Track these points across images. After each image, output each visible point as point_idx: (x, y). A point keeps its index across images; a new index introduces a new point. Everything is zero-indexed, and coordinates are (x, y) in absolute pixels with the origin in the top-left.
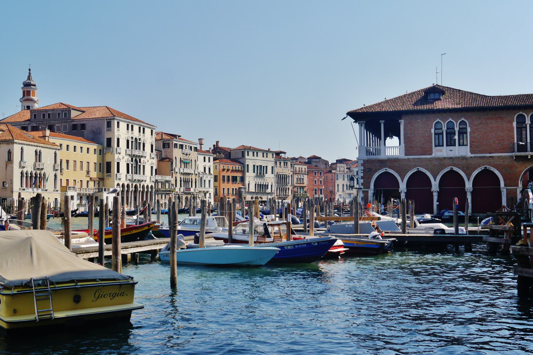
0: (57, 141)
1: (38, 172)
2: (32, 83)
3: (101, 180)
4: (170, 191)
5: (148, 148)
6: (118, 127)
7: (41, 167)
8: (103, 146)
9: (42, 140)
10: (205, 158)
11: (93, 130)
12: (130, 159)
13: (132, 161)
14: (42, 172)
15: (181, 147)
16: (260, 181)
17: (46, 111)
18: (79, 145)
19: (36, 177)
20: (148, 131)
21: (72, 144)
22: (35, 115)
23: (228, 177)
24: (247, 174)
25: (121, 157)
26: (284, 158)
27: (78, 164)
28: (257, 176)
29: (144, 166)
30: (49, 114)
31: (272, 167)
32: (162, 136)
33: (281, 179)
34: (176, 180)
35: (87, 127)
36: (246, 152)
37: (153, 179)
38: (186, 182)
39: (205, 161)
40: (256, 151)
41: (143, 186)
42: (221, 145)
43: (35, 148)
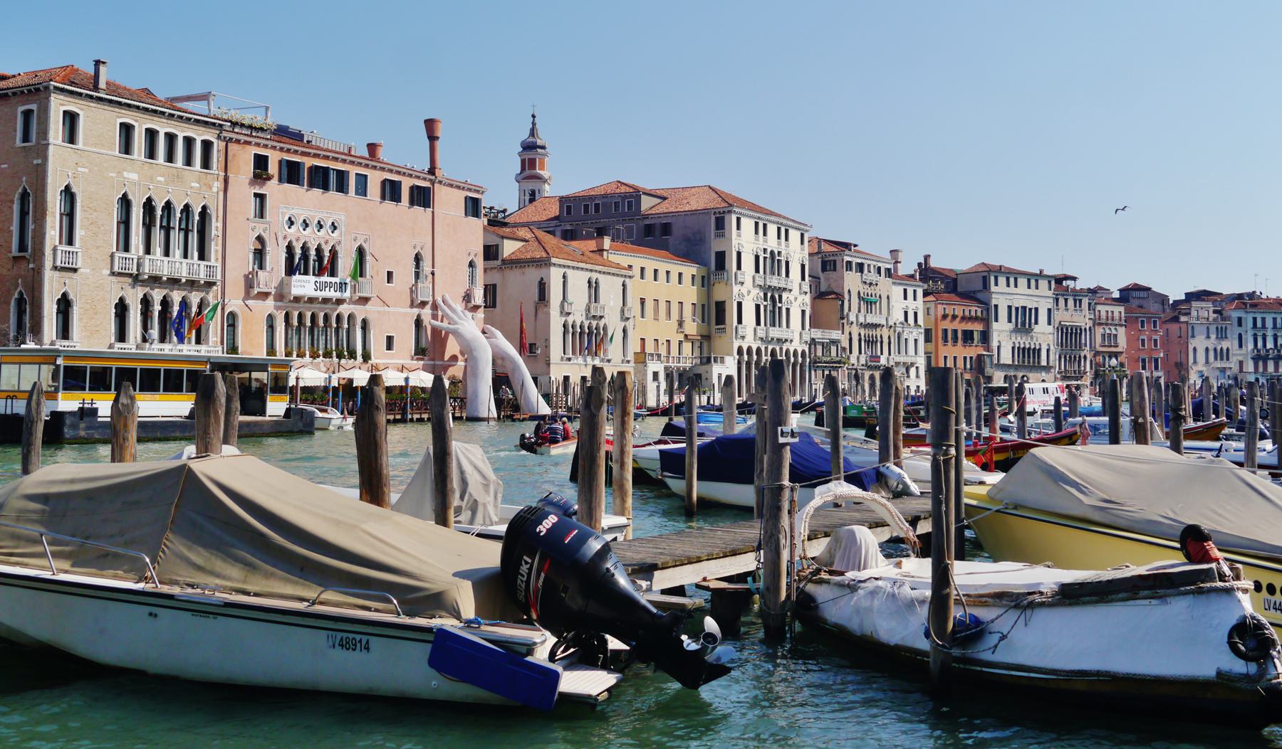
0: (622, 259)
1: (594, 323)
2: (539, 142)
3: (706, 338)
4: (839, 362)
6: (738, 228)
7: (599, 314)
8: (709, 269)
9: (596, 256)
10: (905, 291)
11: (690, 236)
12: (762, 294)
13: (765, 300)
14: (602, 323)
15: (860, 267)
16: (1023, 341)
17: (591, 198)
18: (663, 267)
19: (590, 334)
20: (794, 235)
21: (650, 264)
22: (569, 208)
23: (955, 331)
24: (995, 325)
25: (744, 290)
26: (1074, 290)
27: (662, 306)
28: (1016, 330)
29: (788, 310)
30: (597, 206)
31: (1049, 310)
32: (819, 247)
33: (1069, 336)
34: (851, 340)
35: (677, 230)
36: (992, 279)
37: (807, 338)
38: (871, 342)
39: (905, 298)
40: (1012, 275)
41: (788, 351)
42: (934, 263)
43: (588, 274)
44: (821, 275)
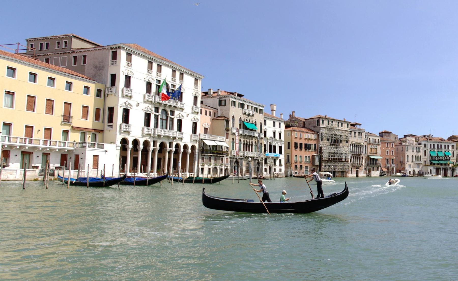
5: (188, 98)
15: (242, 106)
36: (321, 121)
39: (274, 126)
41: (177, 146)
42: (296, 115)
44: (219, 108)
